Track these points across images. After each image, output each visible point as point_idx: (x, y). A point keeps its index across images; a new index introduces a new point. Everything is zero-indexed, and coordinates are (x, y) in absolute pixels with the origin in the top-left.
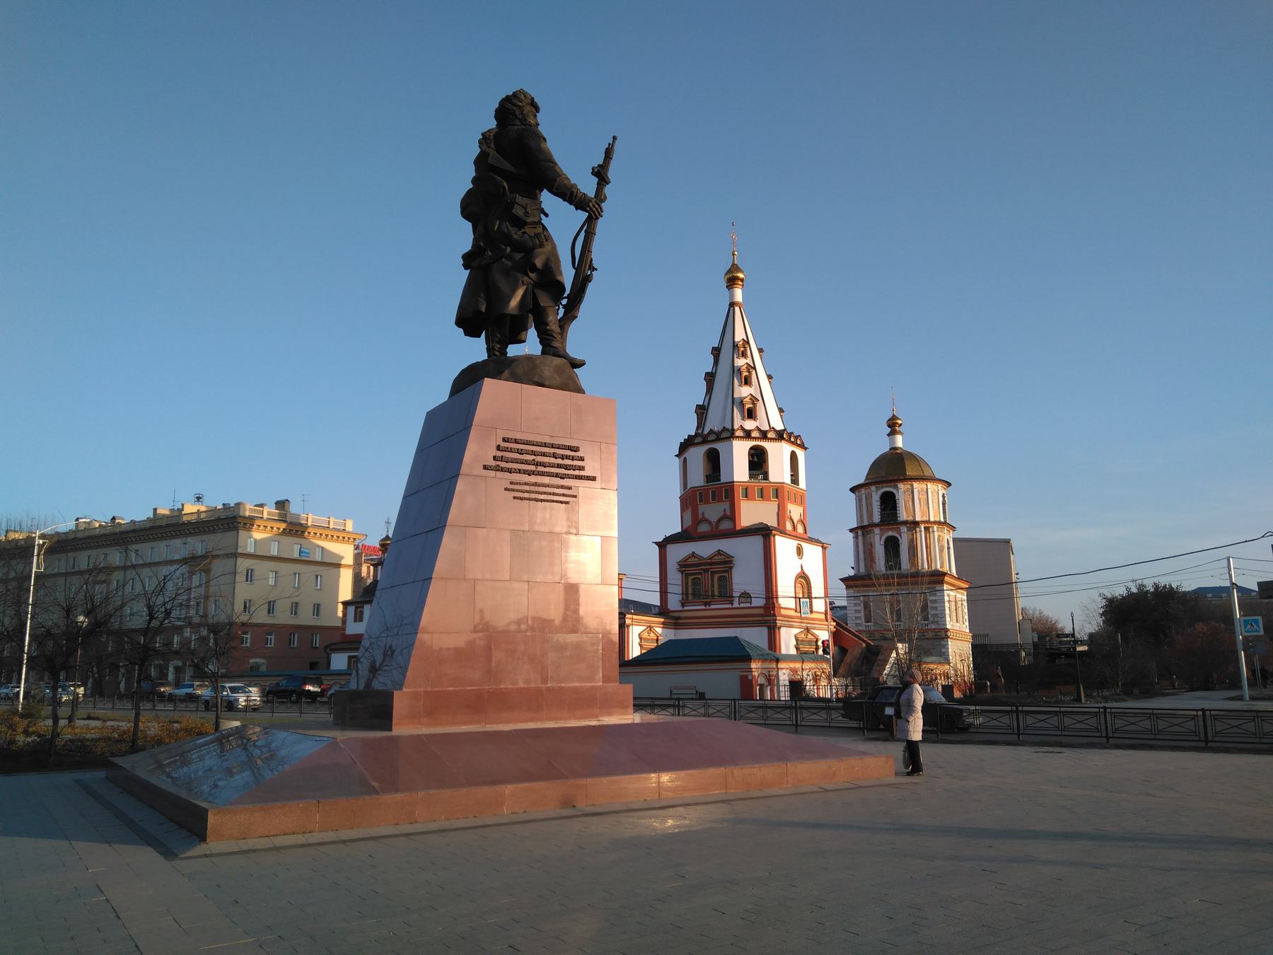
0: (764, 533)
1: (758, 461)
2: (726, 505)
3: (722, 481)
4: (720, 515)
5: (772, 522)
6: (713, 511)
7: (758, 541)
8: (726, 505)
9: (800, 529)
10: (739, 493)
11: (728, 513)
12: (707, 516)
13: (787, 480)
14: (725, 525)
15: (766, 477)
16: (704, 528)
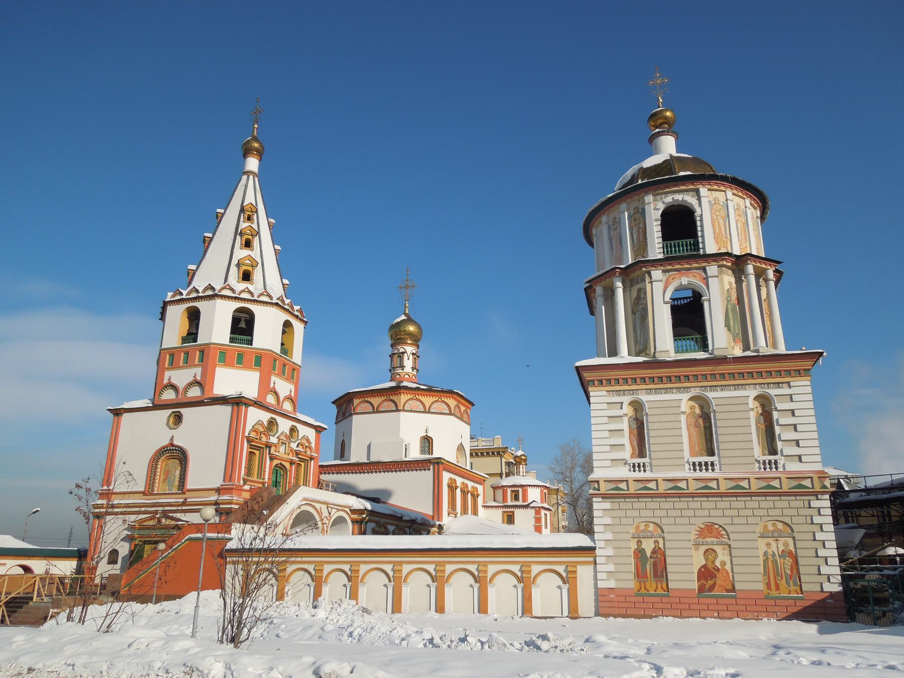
0: (237, 402)
1: (243, 326)
2: (198, 371)
3: (199, 341)
4: (191, 379)
5: (251, 391)
6: (181, 377)
7: (227, 409)
8: (198, 371)
9: (287, 406)
10: (215, 355)
11: (199, 378)
12: (174, 381)
13: (277, 349)
14: (195, 392)
15: (250, 342)
16: (169, 395)
